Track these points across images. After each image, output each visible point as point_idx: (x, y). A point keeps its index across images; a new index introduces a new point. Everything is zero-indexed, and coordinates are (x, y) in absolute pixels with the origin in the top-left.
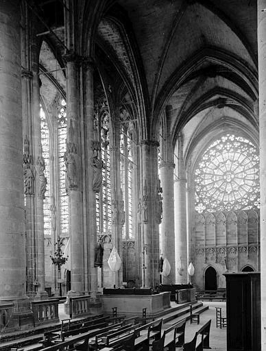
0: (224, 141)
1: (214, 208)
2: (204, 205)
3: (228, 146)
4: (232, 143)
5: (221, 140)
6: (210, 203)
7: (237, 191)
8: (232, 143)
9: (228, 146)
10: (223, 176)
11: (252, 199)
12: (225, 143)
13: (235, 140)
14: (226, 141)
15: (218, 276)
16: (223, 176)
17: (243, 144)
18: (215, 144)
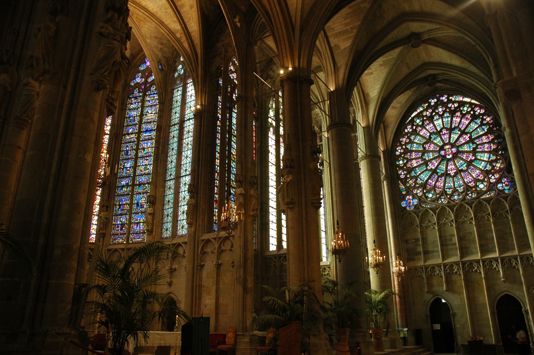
0: (432, 104)
1: (433, 201)
2: (414, 197)
4: (444, 105)
5: (430, 103)
6: (424, 194)
7: (465, 171)
8: (444, 105)
11: (493, 180)
13: (449, 101)
15: (454, 315)
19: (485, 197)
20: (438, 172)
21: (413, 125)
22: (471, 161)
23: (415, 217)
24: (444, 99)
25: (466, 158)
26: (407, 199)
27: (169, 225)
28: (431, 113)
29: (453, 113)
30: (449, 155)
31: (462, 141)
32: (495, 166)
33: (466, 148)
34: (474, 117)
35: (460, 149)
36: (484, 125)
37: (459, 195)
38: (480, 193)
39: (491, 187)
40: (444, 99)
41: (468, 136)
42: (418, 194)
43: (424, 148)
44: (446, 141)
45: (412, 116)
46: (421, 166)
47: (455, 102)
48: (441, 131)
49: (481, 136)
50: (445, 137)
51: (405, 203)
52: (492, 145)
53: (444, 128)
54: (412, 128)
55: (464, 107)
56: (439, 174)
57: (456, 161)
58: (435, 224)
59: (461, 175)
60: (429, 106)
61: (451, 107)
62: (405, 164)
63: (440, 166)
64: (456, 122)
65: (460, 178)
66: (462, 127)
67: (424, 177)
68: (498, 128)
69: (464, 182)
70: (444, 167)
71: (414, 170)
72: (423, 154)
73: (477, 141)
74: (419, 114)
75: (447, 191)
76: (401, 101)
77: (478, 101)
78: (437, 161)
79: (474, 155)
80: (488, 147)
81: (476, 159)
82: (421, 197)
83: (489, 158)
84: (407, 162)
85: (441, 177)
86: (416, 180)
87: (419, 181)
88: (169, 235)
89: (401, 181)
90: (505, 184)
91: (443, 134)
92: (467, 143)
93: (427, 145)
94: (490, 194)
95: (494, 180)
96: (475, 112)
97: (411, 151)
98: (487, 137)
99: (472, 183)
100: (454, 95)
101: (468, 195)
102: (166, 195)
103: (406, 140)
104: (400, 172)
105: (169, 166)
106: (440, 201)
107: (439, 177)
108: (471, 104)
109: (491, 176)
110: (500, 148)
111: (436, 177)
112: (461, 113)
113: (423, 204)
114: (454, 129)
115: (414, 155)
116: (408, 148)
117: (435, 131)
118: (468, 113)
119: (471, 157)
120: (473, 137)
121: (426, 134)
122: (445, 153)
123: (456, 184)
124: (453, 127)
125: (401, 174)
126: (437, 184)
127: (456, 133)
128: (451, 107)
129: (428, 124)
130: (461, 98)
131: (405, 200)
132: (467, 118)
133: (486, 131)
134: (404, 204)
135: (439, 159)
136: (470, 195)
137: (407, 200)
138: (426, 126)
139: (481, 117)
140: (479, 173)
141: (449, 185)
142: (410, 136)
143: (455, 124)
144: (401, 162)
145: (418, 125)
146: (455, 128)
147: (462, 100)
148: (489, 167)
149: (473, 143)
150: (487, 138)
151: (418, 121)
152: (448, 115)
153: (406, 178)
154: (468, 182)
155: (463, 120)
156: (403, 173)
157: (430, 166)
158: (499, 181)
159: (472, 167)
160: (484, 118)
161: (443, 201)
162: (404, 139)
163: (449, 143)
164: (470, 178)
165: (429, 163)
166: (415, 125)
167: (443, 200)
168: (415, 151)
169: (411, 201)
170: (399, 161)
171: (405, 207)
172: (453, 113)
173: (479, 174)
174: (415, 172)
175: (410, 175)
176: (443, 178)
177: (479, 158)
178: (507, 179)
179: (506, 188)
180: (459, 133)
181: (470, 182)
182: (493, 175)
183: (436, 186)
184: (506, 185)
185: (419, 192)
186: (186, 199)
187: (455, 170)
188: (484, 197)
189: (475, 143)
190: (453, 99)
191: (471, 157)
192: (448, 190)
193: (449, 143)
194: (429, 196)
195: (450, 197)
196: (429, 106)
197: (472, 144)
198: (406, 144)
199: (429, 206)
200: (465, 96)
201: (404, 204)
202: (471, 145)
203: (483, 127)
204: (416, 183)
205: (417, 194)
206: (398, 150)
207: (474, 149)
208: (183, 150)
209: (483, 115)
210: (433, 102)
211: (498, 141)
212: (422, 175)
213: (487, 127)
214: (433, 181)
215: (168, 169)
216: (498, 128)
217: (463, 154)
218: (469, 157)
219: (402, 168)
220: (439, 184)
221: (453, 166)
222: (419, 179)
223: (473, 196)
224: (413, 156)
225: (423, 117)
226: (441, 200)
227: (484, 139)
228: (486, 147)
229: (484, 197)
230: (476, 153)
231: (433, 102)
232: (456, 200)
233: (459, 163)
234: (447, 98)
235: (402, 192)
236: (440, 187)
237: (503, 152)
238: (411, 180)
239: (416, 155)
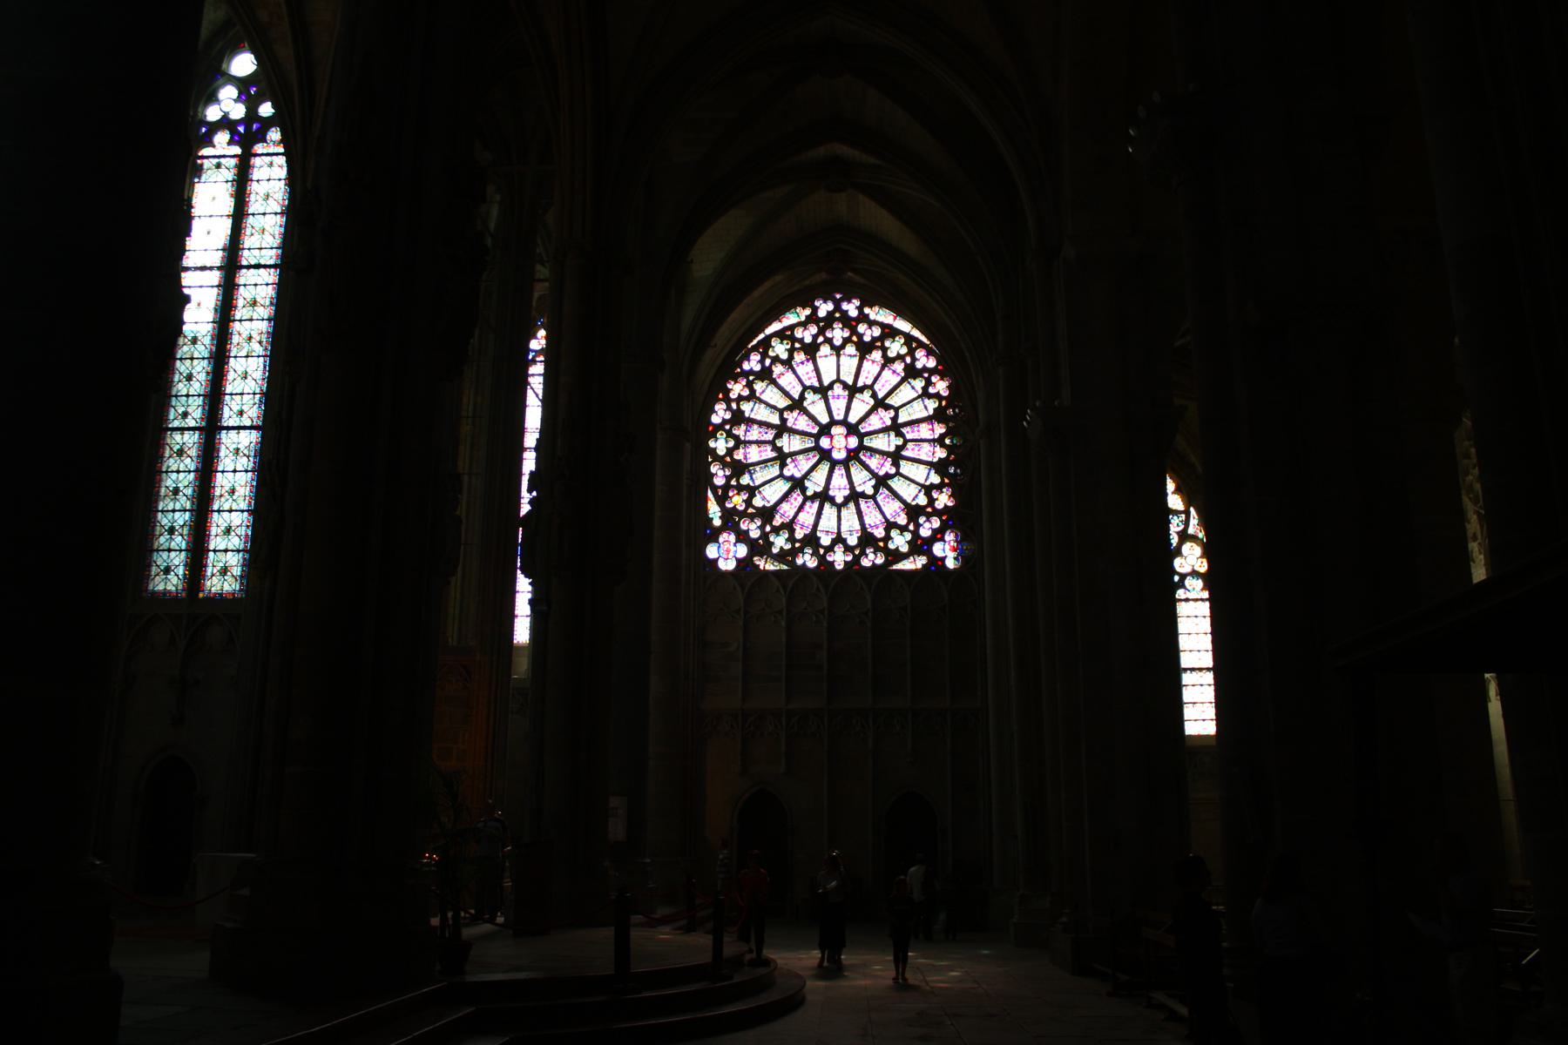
0: (822, 313)
1: (782, 556)
3: (838, 334)
4: (847, 322)
5: (815, 310)
8: (847, 322)
9: (838, 334)
10: (817, 437)
11: (925, 532)
12: (829, 321)
14: (830, 314)
16: (817, 437)
17: (889, 332)
18: (790, 319)
21: (764, 355)
22: (888, 476)
23: (735, 588)
24: (851, 309)
26: (721, 540)
27: (178, 560)
28: (815, 337)
29: (864, 349)
31: (875, 422)
34: (911, 372)
35: (867, 442)
36: (930, 396)
38: (897, 556)
39: (920, 546)
40: (851, 309)
43: (784, 421)
44: (838, 415)
45: (769, 330)
46: (769, 464)
47: (875, 323)
48: (831, 386)
54: (762, 361)
57: (852, 470)
58: (780, 612)
60: (813, 319)
62: (730, 452)
64: (869, 373)
67: (772, 493)
68: (957, 410)
71: (749, 472)
72: (778, 436)
73: (908, 432)
74: (785, 329)
77: (928, 339)
78: (809, 459)
79: (896, 464)
84: (736, 447)
85: (813, 502)
86: (752, 496)
87: (758, 502)
88: (176, 586)
91: (833, 397)
92: (885, 430)
96: (914, 359)
97: (750, 422)
101: (867, 556)
102: (167, 472)
104: (714, 469)
105: (181, 388)
107: (806, 499)
108: (909, 339)
110: (954, 459)
111: (800, 499)
112: (885, 356)
114: (861, 390)
116: (743, 412)
117: (817, 384)
118: (900, 357)
119: (888, 468)
120: (901, 420)
124: (860, 384)
130: (892, 317)
131: (717, 541)
133: (931, 412)
134: (711, 551)
135: (814, 456)
136: (871, 556)
139: (926, 375)
142: (753, 382)
145: (776, 359)
146: (865, 387)
147: (1211, 633)
148: (922, 500)
149: (899, 434)
153: (727, 487)
154: (873, 525)
158: (938, 535)
159: (887, 492)
160: (934, 379)
161: (808, 560)
163: (844, 423)
165: (789, 460)
172: (864, 349)
174: (752, 478)
175: (738, 481)
176: (816, 505)
180: (872, 402)
182: (928, 520)
183: (798, 521)
185: (753, 529)
186: (236, 494)
188: (899, 566)
189: (902, 435)
190: (872, 317)
191: (888, 468)
193: (844, 423)
196: (813, 319)
198: (740, 398)
200: (900, 312)
201: (711, 551)
203: (927, 401)
204: (748, 502)
205: (747, 532)
207: (899, 448)
208: (230, 351)
209: (932, 372)
210: (824, 308)
211: (952, 441)
215: (176, 396)
216: (957, 410)
217: (871, 455)
218: (882, 465)
219: (720, 459)
225: (793, 339)
229: (899, 566)
231: (824, 308)
234: (860, 309)
237: (959, 471)
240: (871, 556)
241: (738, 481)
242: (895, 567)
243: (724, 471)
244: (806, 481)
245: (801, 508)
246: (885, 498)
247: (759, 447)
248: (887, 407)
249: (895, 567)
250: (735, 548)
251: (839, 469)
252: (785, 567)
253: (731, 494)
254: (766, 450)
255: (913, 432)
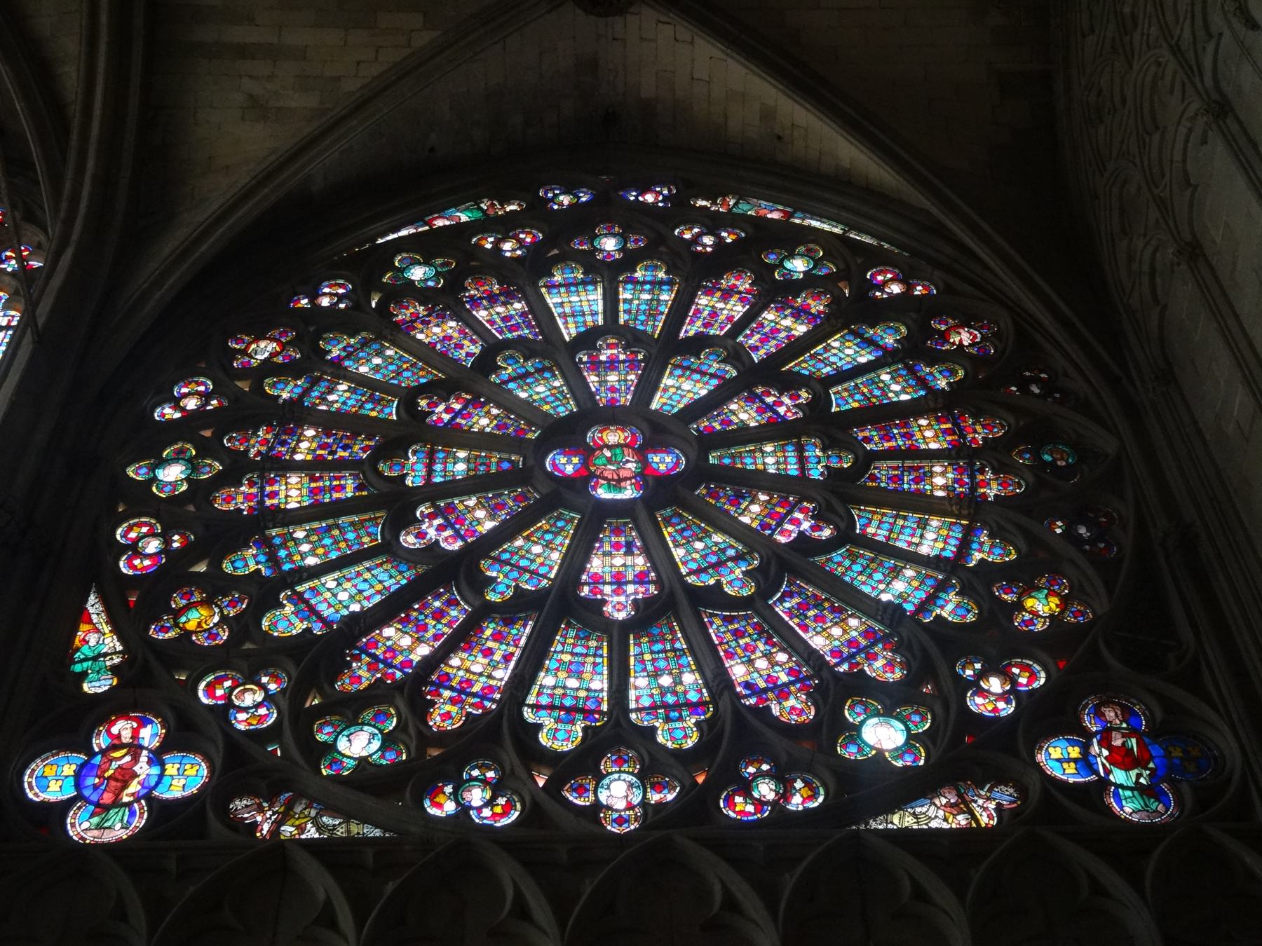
19: (909, 822)
20: (494, 580)
25: (764, 526)
26: (101, 741)
30: (617, 483)
32: (1019, 606)
33: (770, 459)
36: (934, 358)
37: (647, 777)
41: (794, 397)
42: (242, 716)
46: (344, 520)
47: (732, 221)
48: (588, 339)
49: (905, 412)
50: (612, 378)
51: (69, 770)
52: (989, 475)
53: (611, 327)
55: (791, 256)
56: (493, 597)
57: (667, 532)
59: (704, 628)
61: (696, 240)
62: (199, 491)
63: (519, 542)
65: (681, 644)
66: (756, 349)
69: (718, 681)
70: (556, 556)
71: (266, 543)
75: (539, 727)
76: (338, 79)
80: (955, 481)
81: (847, 537)
82: (259, 737)
83: (964, 547)
84: (230, 477)
85: (509, 622)
89: (105, 600)
90: (1105, 742)
91: (595, 365)
93: (441, 408)
94: (963, 805)
95: (1006, 709)
98: (949, 426)
99: (792, 702)
100: (724, 195)
101: (746, 788)
103: (273, 355)
106: (450, 807)
109: (982, 675)
113: (261, 810)
115: (306, 446)
121: (461, 346)
122: (586, 463)
123: (640, 689)
125: (134, 549)
126: (455, 661)
127: (703, 374)
128: (696, 240)
129: (492, 299)
132: (798, 314)
137: (104, 752)
138: (475, 302)
140: (867, 633)
141: (573, 683)
143: (706, 325)
144: (173, 473)
150: (945, 432)
151: (417, 274)
152: (661, 275)
154: (762, 684)
155: (769, 316)
156: (153, 546)
157: (432, 533)
162: (262, 344)
164: (782, 657)
165: (423, 509)
166: (381, 288)
167: (476, 796)
168: (331, 422)
169: (143, 768)
170: (163, 463)
171: (46, 805)
173: (863, 642)
176: (522, 632)
177: (875, 530)
178: (1128, 714)
179: (1118, 776)
181: (782, 693)
184: (1123, 759)
187: (652, 589)
188: (901, 820)
189: (852, 446)
192: (547, 720)
194: (342, 744)
195: (554, 787)
197: (824, 450)
198: (268, 367)
199: (312, 833)
202: (814, 452)
206: (185, 396)
211: (1037, 456)
212: (329, 581)
213: (953, 373)
214: (419, 640)
220: (477, 668)
221: (640, 561)
222: (289, 609)
223: (796, 803)
224: (294, 451)
226: (455, 795)
227: (929, 435)
228: (939, 481)
229: (901, 820)
230: (858, 502)
232: (620, 821)
233: (699, 545)
235: (84, 675)
236: (476, 688)
238: (208, 603)
239: (322, 446)
240: (766, 790)
241: (216, 565)
242: (877, 825)
243: (167, 542)
244: (484, 564)
245: (462, 638)
246: (803, 607)
247: (313, 479)
248: (790, 383)
249: (877, 825)
250: (155, 771)
251: (617, 531)
252: (377, 833)
253: (178, 602)
254: (342, 488)
255: (887, 437)
